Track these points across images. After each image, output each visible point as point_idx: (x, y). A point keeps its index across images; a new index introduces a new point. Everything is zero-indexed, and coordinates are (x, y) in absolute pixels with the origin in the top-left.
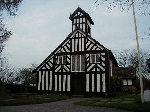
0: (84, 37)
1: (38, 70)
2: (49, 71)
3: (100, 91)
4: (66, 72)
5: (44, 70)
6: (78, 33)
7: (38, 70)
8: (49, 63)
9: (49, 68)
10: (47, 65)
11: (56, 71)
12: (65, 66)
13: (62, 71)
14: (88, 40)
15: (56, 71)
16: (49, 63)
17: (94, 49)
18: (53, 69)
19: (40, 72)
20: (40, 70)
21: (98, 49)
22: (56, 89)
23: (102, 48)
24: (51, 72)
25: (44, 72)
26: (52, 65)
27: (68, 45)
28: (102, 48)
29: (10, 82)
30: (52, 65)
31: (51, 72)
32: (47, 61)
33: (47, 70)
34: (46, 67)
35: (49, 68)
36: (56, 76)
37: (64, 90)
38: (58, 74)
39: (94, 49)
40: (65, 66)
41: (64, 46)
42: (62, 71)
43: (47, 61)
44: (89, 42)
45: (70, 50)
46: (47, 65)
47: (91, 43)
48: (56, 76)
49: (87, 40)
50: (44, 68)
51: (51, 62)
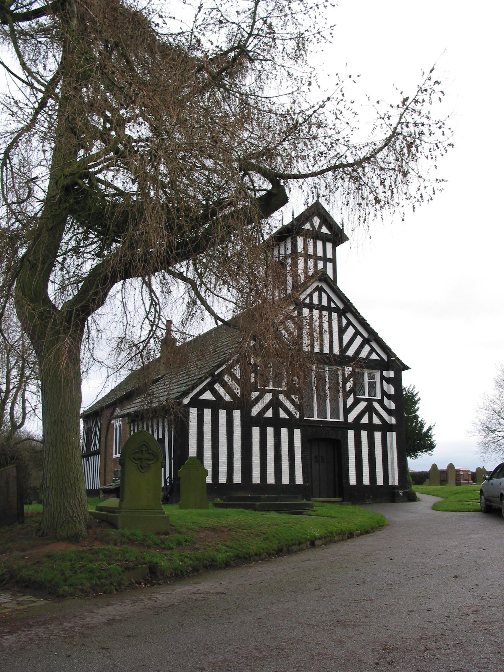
1: (186, 401)
5: (207, 404)
6: (320, 290)
9: (227, 398)
10: (217, 386)
11: (255, 411)
13: (276, 413)
14: (349, 323)
15: (255, 411)
17: (364, 354)
18: (244, 404)
19: (193, 412)
21: (374, 356)
23: (385, 357)
24: (237, 415)
25: (207, 413)
28: (385, 357)
34: (215, 392)
35: (227, 398)
36: (256, 431)
38: (262, 422)
39: (364, 354)
42: (276, 413)
44: (350, 331)
46: (217, 386)
47: (357, 333)
48: (256, 431)
49: (344, 322)
50: (208, 396)
51: (233, 377)
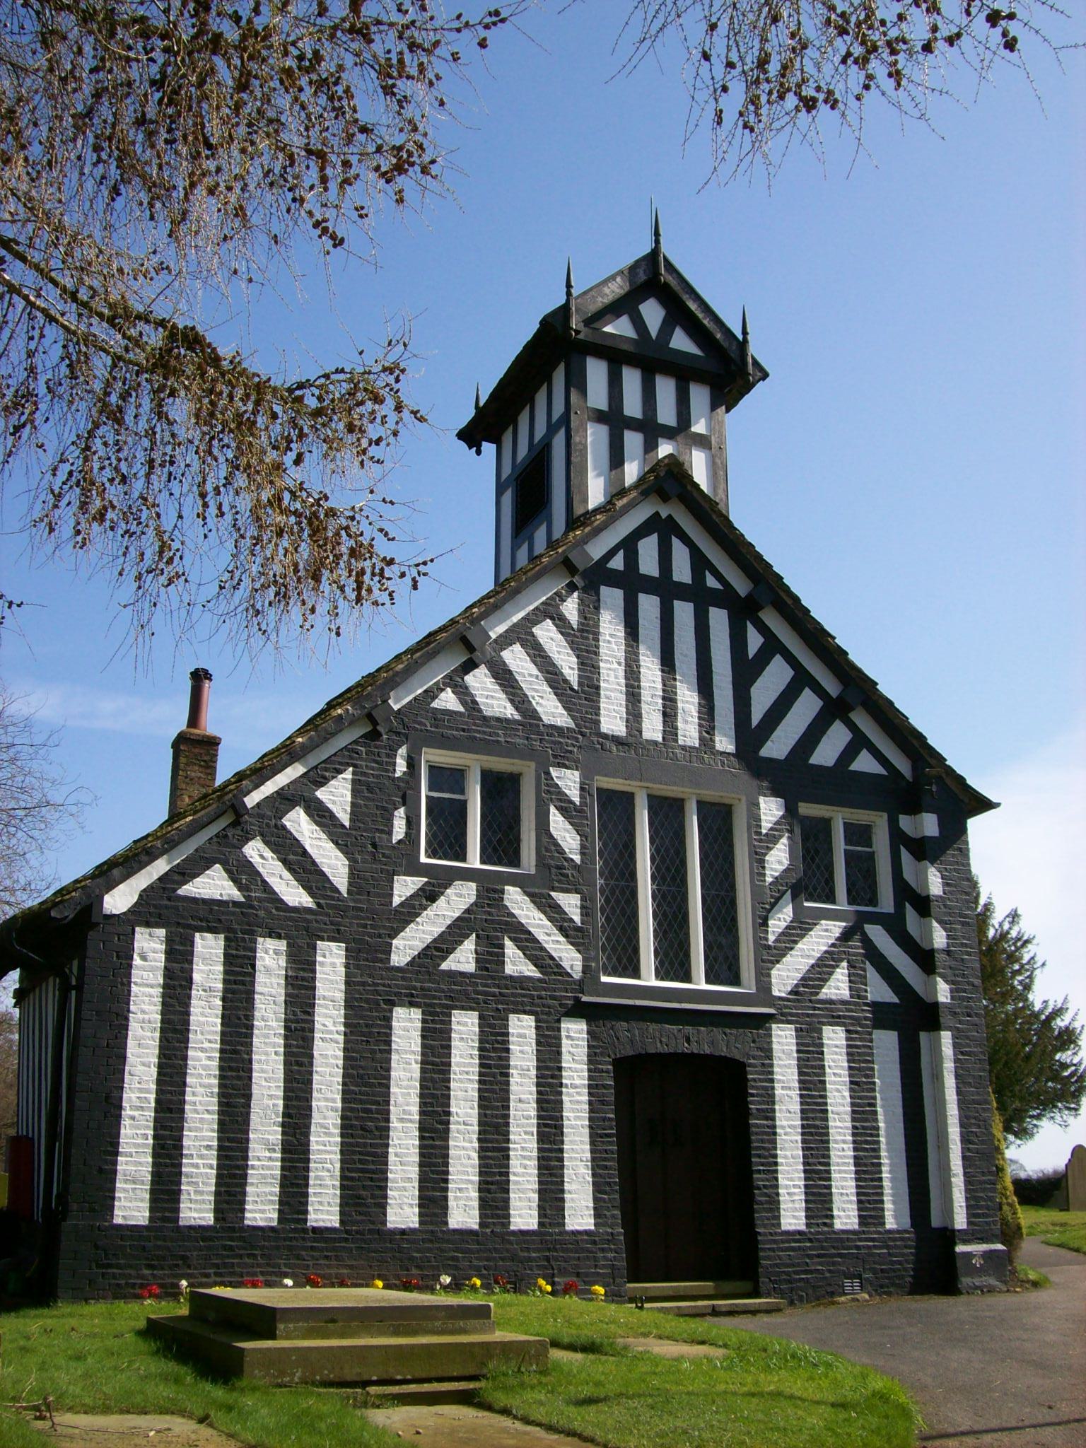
0: (726, 598)
1: (119, 900)
2: (301, 935)
3: (208, 1218)
4: (530, 970)
5: (211, 915)
6: (664, 529)
7: (119, 900)
8: (299, 823)
9: (294, 895)
10: (256, 851)
11: (406, 946)
12: (517, 902)
13: (490, 959)
14: (772, 647)
15: (406, 946)
16: (299, 823)
17: (826, 753)
18: (361, 919)
19: (150, 947)
20: (152, 908)
21: (864, 763)
22: (402, 1211)
23: (903, 765)
24: (331, 961)
25: (209, 951)
26: (334, 864)
27: (546, 633)
28: (903, 765)
29: (150, 1291)
30: (334, 864)
31: (331, 961)
32: (269, 788)
33: (243, 923)
34: (243, 873)
35: (294, 895)
36: (406, 1026)
37: (463, 1212)
38: (432, 989)
39: (826, 753)
40: (517, 902)
41: (505, 641)
42: (490, 959)
43: (269, 788)
44: (775, 677)
45: (581, 698)
46: (256, 851)
47: (801, 680)
48: (406, 1026)
49: (754, 641)
50: (214, 885)
51: (321, 815)
